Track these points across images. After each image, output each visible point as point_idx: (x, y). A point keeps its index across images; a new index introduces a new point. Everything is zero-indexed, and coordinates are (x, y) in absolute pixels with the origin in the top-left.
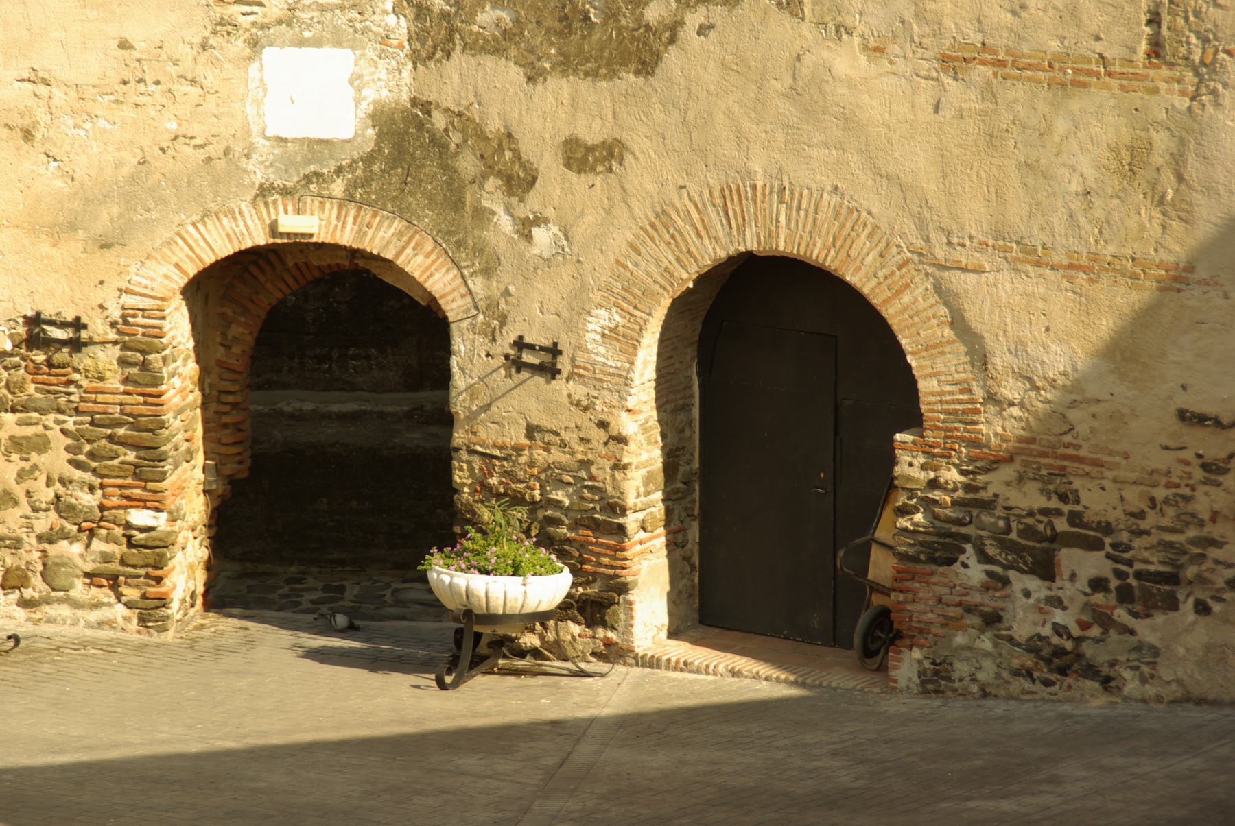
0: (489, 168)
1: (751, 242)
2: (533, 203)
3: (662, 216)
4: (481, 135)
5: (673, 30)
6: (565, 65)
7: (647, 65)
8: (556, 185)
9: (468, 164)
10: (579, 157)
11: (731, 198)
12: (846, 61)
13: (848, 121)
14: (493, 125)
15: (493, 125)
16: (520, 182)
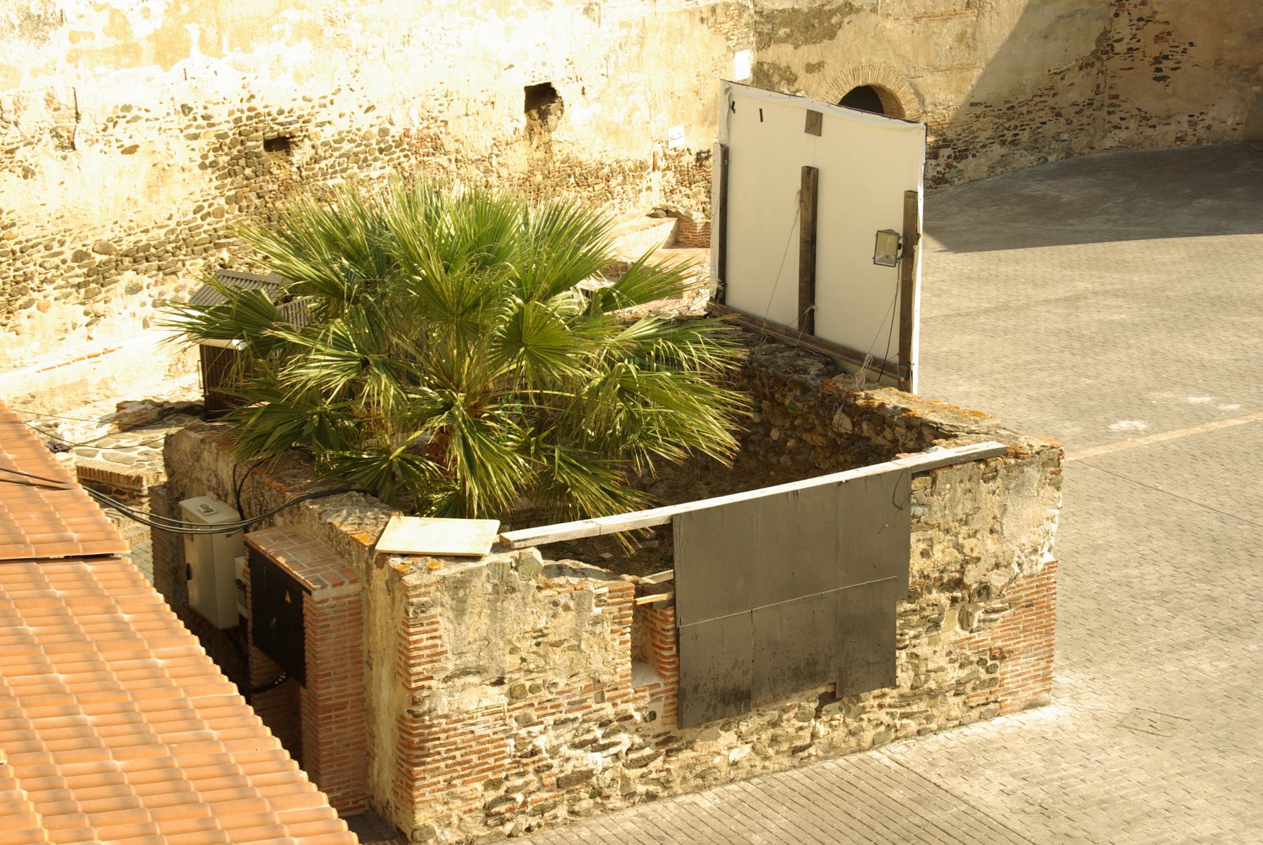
0: (782, 78)
1: (860, 84)
2: (796, 85)
3: (835, 80)
4: (779, 69)
5: (840, 25)
6: (806, 42)
7: (831, 35)
8: (803, 79)
9: (776, 79)
10: (810, 68)
11: (855, 72)
12: (889, 24)
13: (889, 41)
14: (783, 65)
15: (783, 65)
16: (792, 80)
